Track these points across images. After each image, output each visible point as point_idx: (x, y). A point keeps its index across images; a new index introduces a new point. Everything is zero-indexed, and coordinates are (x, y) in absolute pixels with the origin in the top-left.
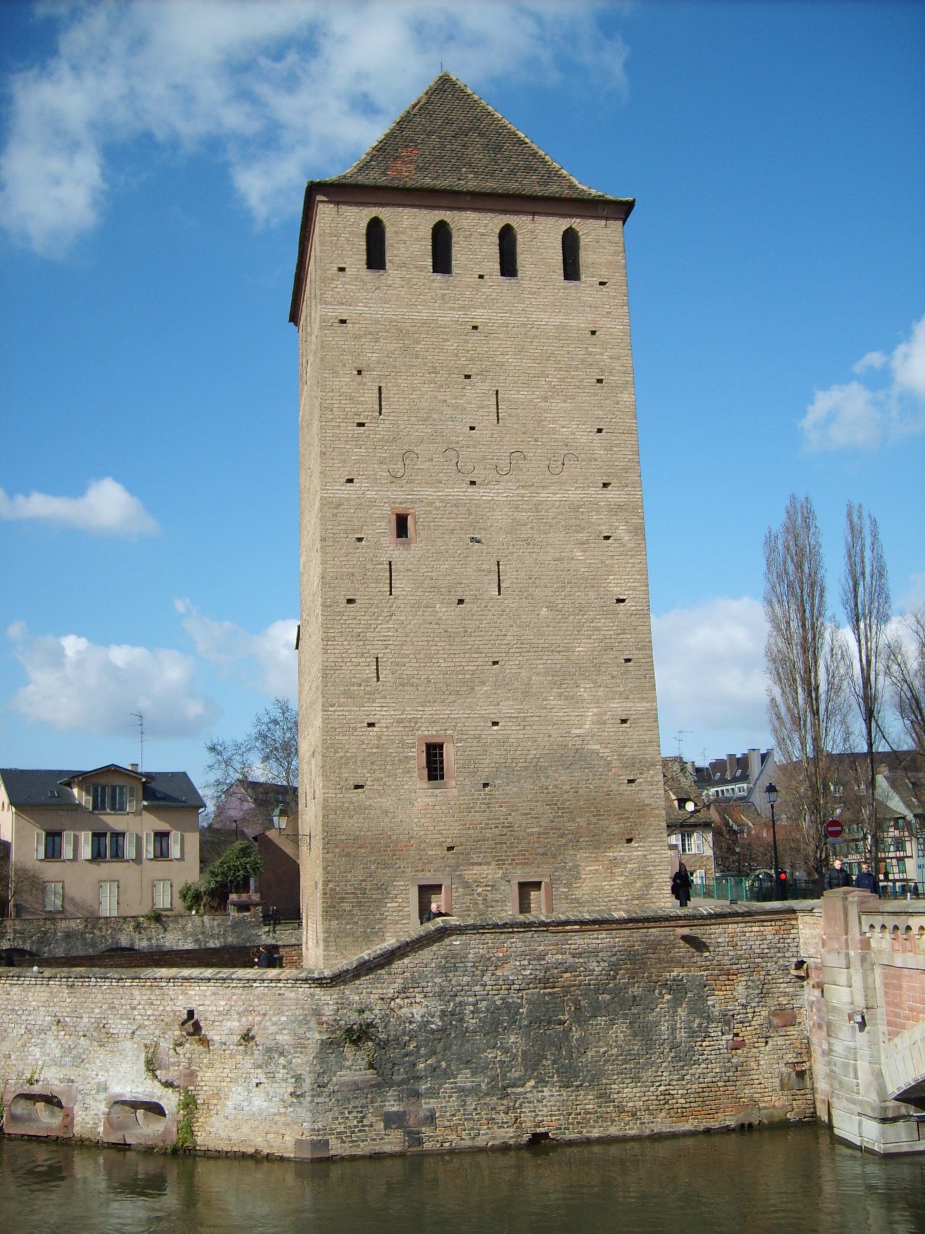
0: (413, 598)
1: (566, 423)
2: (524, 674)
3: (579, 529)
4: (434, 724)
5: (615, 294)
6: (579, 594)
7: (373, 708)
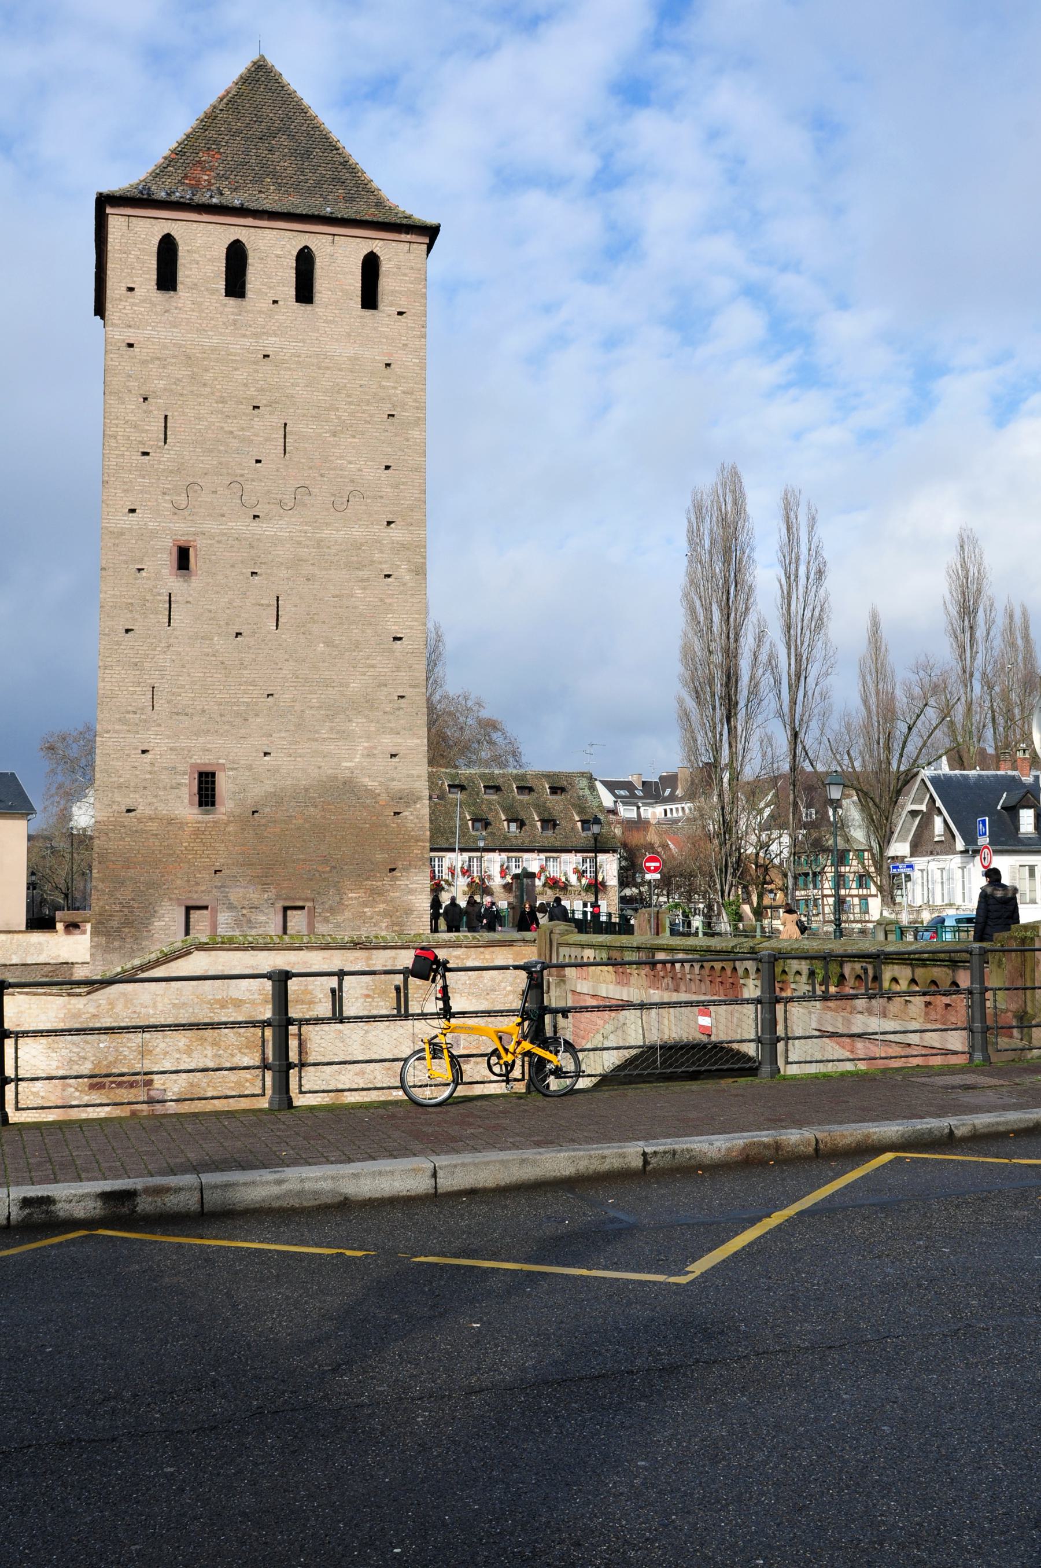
1: (354, 459)
2: (298, 707)
4: (207, 753)
6: (356, 631)
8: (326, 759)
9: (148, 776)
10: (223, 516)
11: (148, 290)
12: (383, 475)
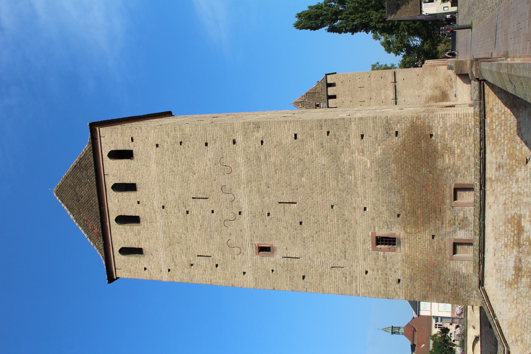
0: (300, 247)
1: (204, 163)
2: (338, 192)
3: (258, 159)
5: (136, 133)
7: (358, 271)
10: (241, 231)
11: (144, 262)
12: (210, 147)
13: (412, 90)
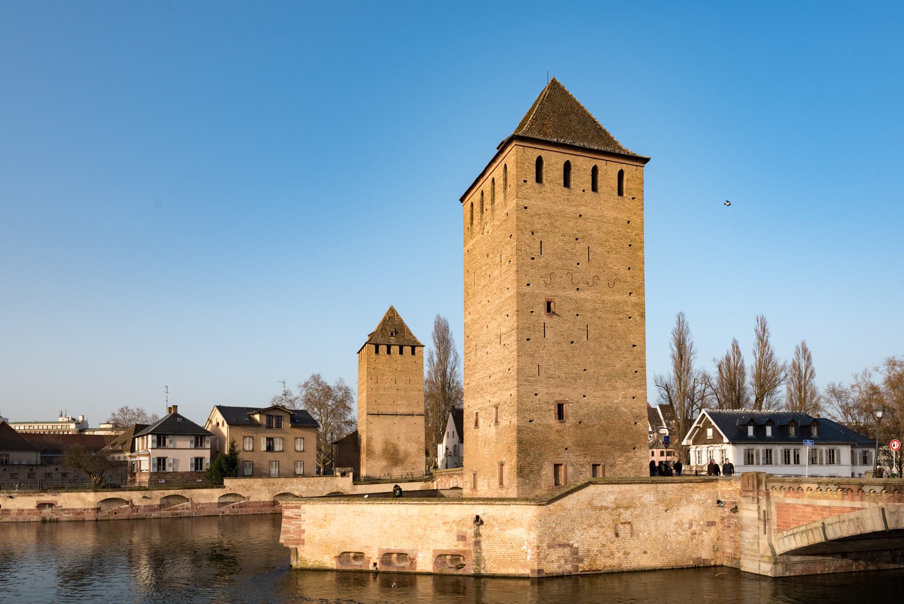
8: (608, 399)
9: (538, 406)
13: (405, 432)
